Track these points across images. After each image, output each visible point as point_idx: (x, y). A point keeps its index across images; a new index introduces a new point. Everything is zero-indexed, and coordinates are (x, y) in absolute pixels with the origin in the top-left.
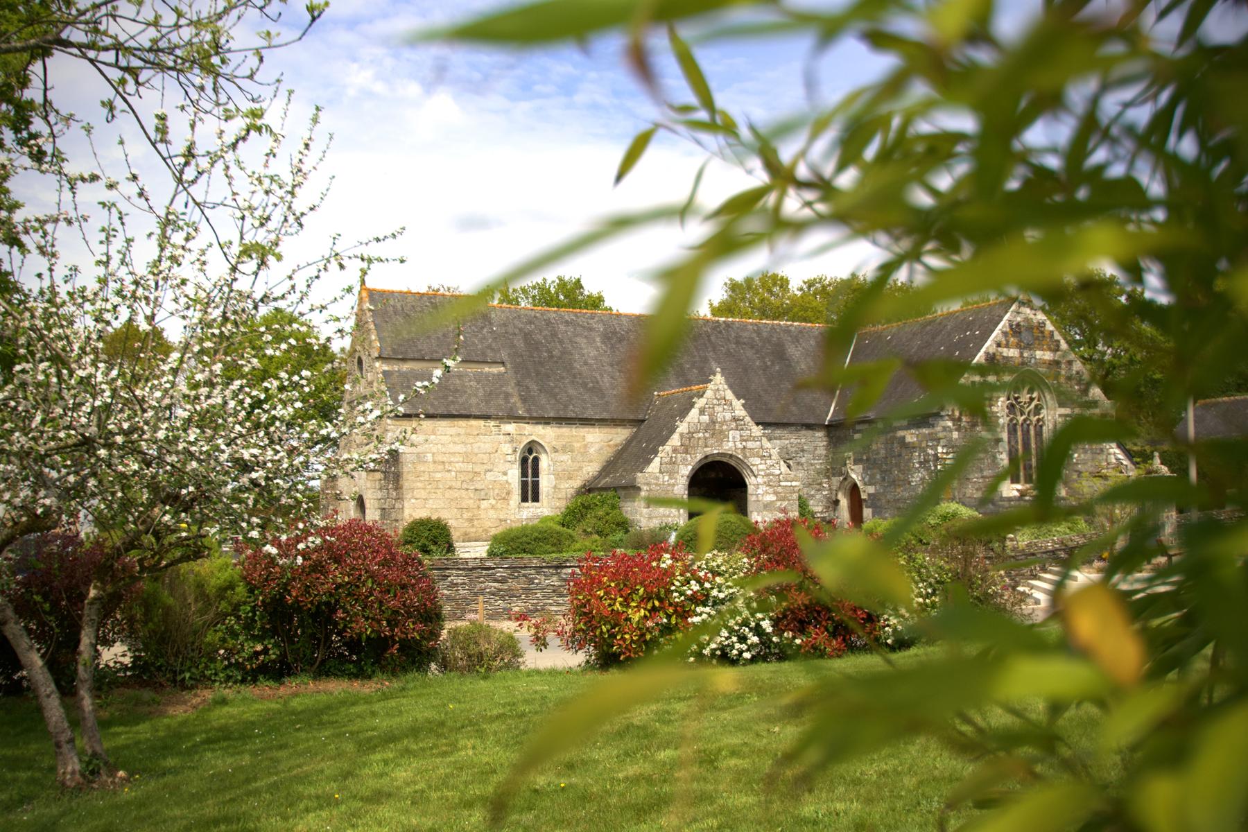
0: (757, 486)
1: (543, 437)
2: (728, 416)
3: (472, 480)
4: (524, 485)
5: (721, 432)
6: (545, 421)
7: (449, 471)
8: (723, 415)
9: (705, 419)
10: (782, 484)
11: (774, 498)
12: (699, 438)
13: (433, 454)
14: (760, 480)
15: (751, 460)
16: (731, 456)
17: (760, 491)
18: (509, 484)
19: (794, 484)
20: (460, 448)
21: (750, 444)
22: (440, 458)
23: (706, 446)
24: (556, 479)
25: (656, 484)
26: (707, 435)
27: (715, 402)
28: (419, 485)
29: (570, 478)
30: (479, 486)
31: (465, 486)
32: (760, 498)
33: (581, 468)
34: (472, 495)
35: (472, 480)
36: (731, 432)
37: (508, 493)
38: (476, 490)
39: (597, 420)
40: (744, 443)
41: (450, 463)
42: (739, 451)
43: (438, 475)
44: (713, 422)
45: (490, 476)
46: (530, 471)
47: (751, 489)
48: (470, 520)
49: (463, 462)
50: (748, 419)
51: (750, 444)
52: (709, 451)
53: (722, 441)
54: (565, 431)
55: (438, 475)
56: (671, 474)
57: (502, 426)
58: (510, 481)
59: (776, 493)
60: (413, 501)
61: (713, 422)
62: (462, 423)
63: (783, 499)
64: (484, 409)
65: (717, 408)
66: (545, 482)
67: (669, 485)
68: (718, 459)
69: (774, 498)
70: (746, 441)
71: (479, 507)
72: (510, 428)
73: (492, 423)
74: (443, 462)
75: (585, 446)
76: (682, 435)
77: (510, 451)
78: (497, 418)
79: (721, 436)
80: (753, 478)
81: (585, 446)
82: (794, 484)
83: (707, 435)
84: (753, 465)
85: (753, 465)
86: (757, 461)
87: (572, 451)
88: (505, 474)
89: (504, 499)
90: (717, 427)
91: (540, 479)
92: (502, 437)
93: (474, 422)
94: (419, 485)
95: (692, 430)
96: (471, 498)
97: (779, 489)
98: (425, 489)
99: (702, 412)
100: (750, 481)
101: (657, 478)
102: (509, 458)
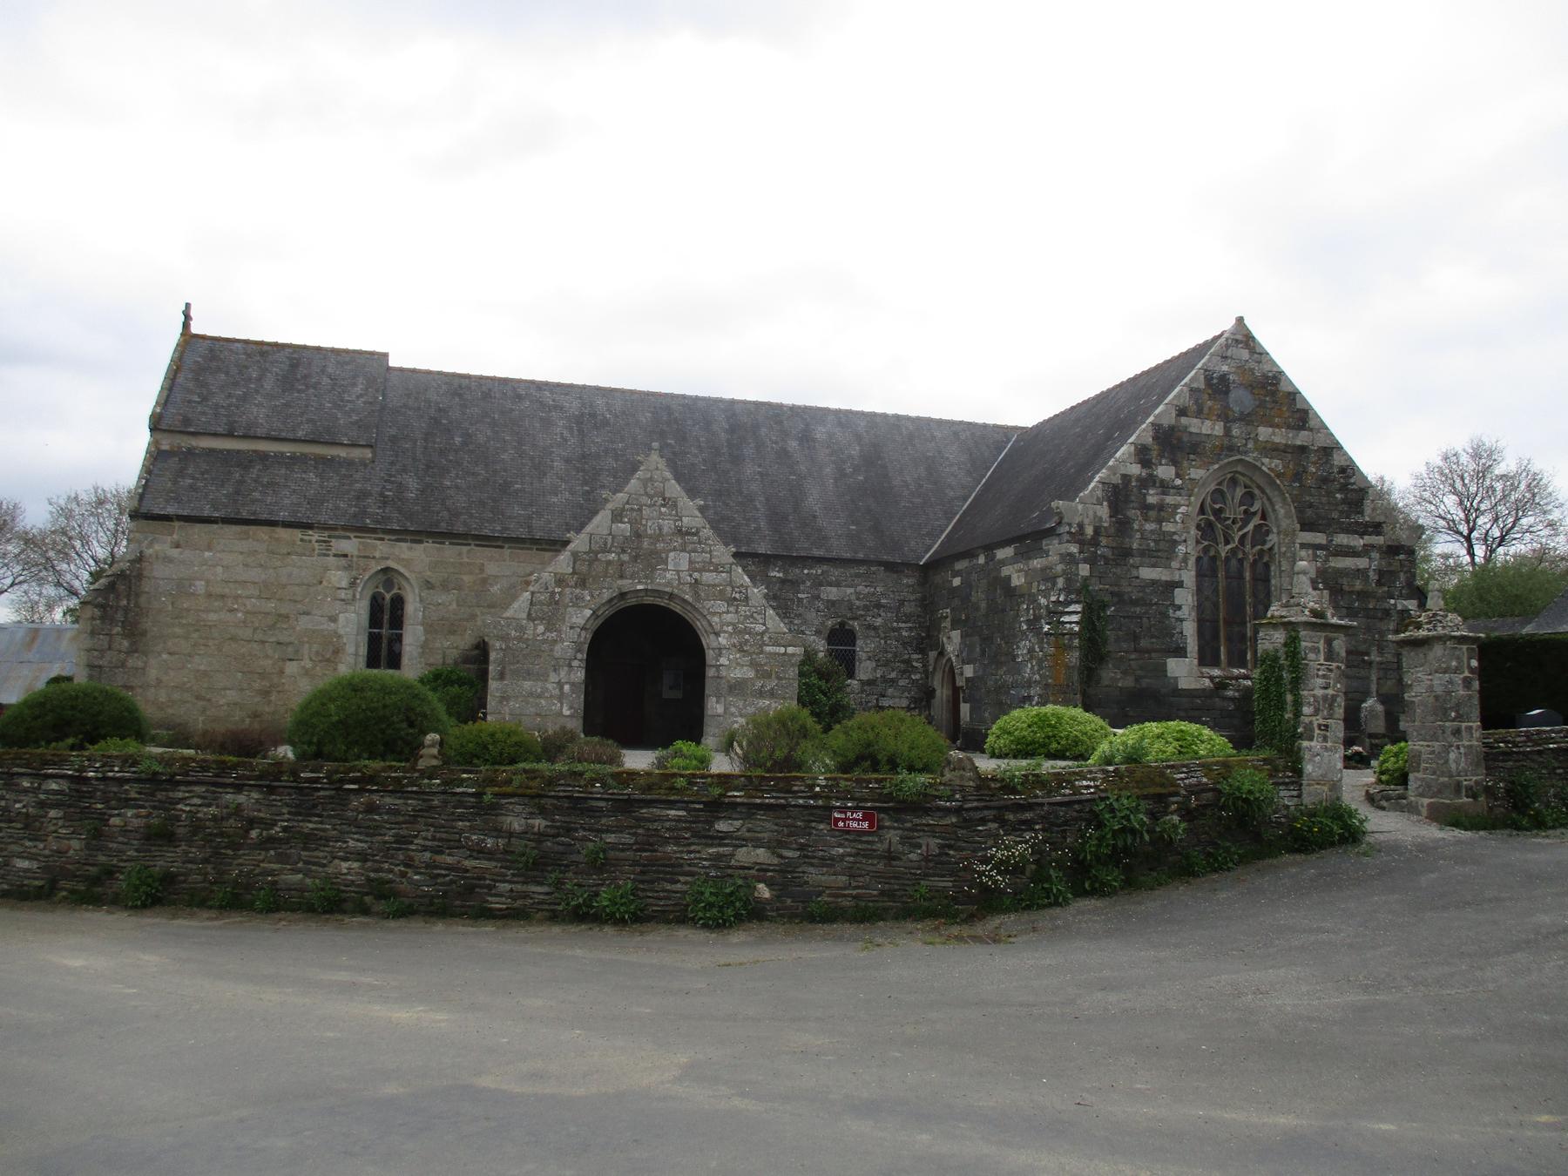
0: (720, 651)
1: (407, 563)
2: (668, 525)
3: (272, 627)
4: (374, 641)
5: (654, 553)
6: (402, 535)
7: (232, 611)
8: (657, 521)
9: (624, 528)
10: (768, 649)
11: (751, 674)
12: (609, 563)
13: (208, 582)
14: (723, 640)
15: (708, 604)
16: (671, 596)
17: (723, 661)
18: (340, 636)
19: (790, 650)
20: (255, 574)
21: (708, 577)
22: (218, 590)
23: (621, 577)
24: (426, 632)
25: (520, 639)
26: (625, 557)
27: (645, 500)
28: (178, 630)
29: (453, 632)
30: (283, 639)
31: (259, 636)
32: (723, 673)
33: (473, 617)
34: (270, 652)
35: (272, 627)
36: (672, 554)
37: (336, 652)
38: (279, 643)
39: (477, 537)
40: (696, 575)
41: (237, 597)
42: (687, 588)
43: (213, 617)
44: (638, 535)
45: (304, 623)
46: (386, 617)
47: (710, 654)
48: (265, 693)
49: (259, 597)
50: (707, 532)
51: (708, 577)
52: (626, 584)
53: (654, 569)
54: (450, 552)
55: (213, 617)
56: (551, 622)
57: (334, 542)
58: (341, 632)
59: (753, 664)
60: (165, 656)
61: (638, 535)
62: (262, 532)
63: (767, 675)
64: (303, 514)
65: (646, 512)
66: (412, 637)
67: (544, 641)
68: (649, 600)
69: (751, 674)
70: (700, 571)
71: (282, 672)
72: (350, 545)
73: (314, 536)
74: (223, 596)
75: (484, 581)
76: (575, 555)
77: (344, 584)
78: (324, 527)
79: (654, 560)
80: (712, 637)
81: (484, 581)
82: (790, 650)
83: (625, 557)
84: (714, 614)
85: (714, 614)
86: (721, 606)
87: (459, 588)
88: (333, 619)
89: (328, 660)
90: (645, 545)
91: (404, 632)
92: (331, 559)
93: (282, 533)
94: (178, 630)
95: (595, 547)
96: (267, 656)
97: (762, 659)
98: (186, 638)
99: (617, 516)
100: (708, 641)
101: (522, 629)
102: (342, 594)
